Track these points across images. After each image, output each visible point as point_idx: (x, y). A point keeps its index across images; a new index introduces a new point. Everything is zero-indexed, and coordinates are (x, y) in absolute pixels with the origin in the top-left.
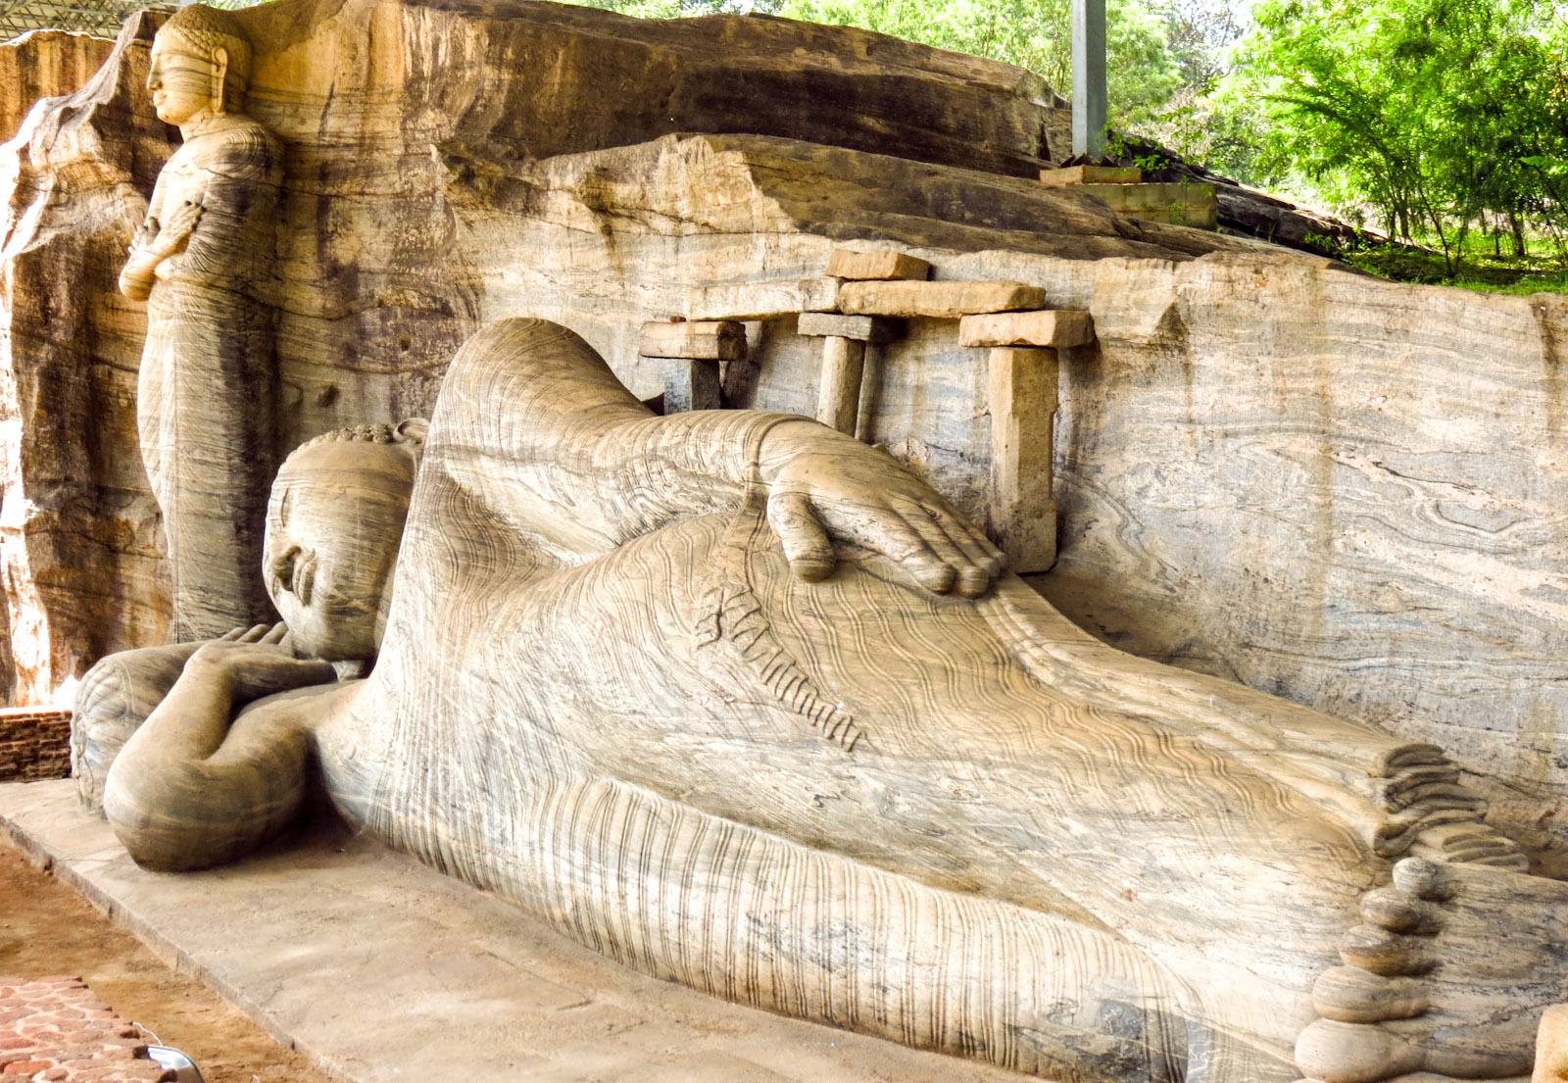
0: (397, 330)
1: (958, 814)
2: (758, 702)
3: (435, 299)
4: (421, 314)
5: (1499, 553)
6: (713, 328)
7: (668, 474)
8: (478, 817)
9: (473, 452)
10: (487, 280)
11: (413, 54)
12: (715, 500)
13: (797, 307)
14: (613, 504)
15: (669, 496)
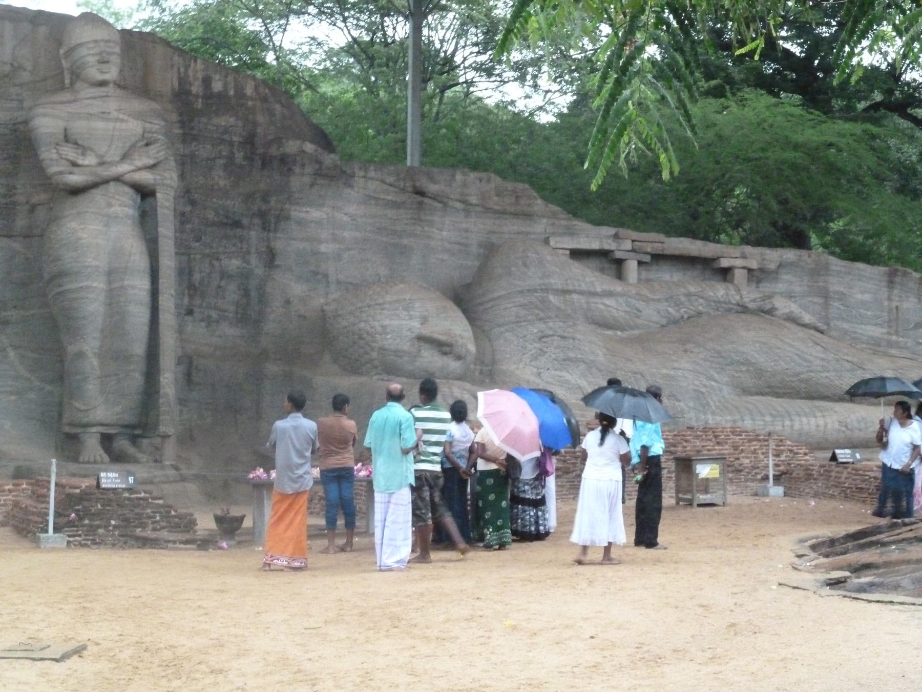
0: (192, 230)
2: (838, 360)
3: (227, 218)
4: (213, 224)
5: (876, 325)
6: (568, 252)
7: (701, 301)
8: (690, 419)
10: (293, 214)
11: (180, 78)
14: (667, 311)
15: (700, 308)
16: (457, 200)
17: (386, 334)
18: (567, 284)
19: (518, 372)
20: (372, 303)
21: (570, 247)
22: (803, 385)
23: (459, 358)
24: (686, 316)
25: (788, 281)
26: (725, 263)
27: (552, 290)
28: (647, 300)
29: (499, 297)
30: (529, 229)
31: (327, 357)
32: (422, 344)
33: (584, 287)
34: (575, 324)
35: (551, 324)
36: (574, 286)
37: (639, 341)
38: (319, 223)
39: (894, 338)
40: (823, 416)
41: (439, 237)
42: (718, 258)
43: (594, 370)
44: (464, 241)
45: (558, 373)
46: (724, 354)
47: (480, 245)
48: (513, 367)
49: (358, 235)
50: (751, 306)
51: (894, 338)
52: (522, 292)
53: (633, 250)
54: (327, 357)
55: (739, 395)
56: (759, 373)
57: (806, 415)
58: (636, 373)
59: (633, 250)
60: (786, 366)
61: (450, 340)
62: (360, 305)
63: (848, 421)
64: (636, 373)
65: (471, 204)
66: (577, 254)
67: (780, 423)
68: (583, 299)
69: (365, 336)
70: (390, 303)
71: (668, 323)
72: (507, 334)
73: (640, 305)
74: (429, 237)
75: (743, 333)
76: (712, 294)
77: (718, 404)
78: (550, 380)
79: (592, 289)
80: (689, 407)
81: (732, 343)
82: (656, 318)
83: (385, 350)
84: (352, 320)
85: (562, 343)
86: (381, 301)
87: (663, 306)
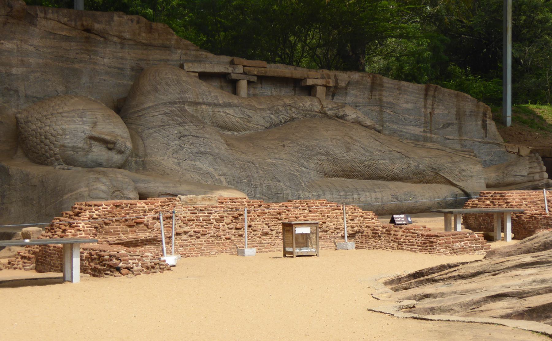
1: (429, 167)
2: (390, 151)
5: (416, 126)
6: (197, 74)
7: (294, 110)
8: (288, 194)
9: (197, 104)
12: (308, 116)
13: (230, 70)
14: (270, 117)
15: (294, 115)
16: (114, 36)
17: (66, 135)
18: (198, 98)
19: (162, 162)
20: (53, 112)
21: (199, 70)
22: (367, 169)
23: (120, 152)
24: (283, 121)
25: (354, 95)
26: (310, 82)
27: (187, 102)
28: (255, 109)
29: (149, 107)
30: (169, 57)
31: (20, 153)
32: (92, 142)
33: (210, 100)
34: (204, 127)
35: (187, 127)
36: (203, 99)
37: (249, 139)
38: (10, 52)
39: (429, 135)
40: (381, 191)
41: (103, 63)
42: (305, 78)
43: (219, 161)
44: (121, 66)
45: (193, 162)
46: (311, 148)
47: (132, 69)
48: (159, 159)
49: (41, 61)
50: (329, 113)
51: (429, 135)
52: (165, 104)
53: (244, 73)
54: (20, 153)
55: (321, 177)
56: (335, 161)
57: (369, 191)
58: (249, 162)
59: (244, 73)
60: (354, 156)
61: (113, 139)
62: (45, 113)
63: (398, 194)
64: (249, 162)
65: (125, 39)
66: (204, 76)
67: (350, 197)
68: (210, 109)
69: (50, 136)
70: (68, 112)
71: (271, 126)
72: (155, 134)
73: (250, 113)
74: (95, 63)
75: (324, 133)
76: (301, 105)
77: (307, 183)
78: (187, 168)
79: (216, 102)
80: (286, 186)
81: (317, 140)
82: (262, 122)
83: (64, 146)
84: (39, 124)
85: (196, 141)
86: (60, 111)
87: (266, 114)
